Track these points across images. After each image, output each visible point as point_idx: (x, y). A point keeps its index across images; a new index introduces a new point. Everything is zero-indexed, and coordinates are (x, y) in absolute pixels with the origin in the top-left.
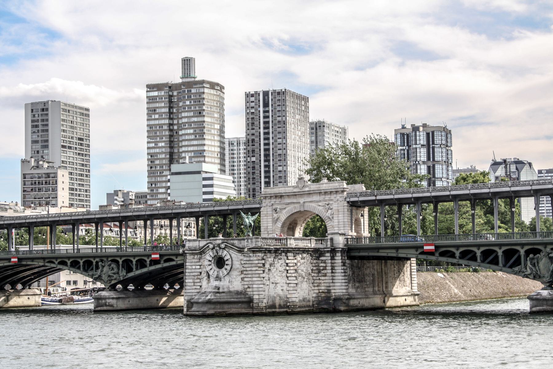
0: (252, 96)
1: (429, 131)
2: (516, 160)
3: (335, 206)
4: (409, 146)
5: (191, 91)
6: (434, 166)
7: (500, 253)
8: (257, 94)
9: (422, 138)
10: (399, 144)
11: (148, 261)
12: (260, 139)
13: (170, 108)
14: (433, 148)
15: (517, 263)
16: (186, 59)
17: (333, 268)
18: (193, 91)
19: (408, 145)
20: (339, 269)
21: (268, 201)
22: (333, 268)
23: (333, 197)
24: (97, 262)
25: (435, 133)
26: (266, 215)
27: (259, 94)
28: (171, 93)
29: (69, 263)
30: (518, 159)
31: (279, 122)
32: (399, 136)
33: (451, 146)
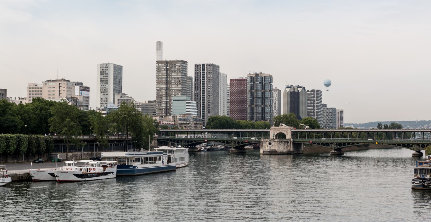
0: (198, 65)
1: (263, 76)
2: (298, 86)
3: (288, 132)
4: (254, 83)
5: (176, 64)
6: (265, 92)
7: (325, 143)
8: (200, 65)
9: (260, 80)
10: (249, 81)
11: (244, 142)
12: (201, 84)
13: (167, 71)
14: (265, 84)
15: (328, 145)
16: (158, 42)
17: (291, 145)
18: (177, 64)
19: (253, 82)
20: (292, 146)
21: (272, 130)
22: (291, 145)
23: (288, 130)
24: (230, 142)
25: (266, 77)
26: (272, 133)
27: (201, 65)
28: (167, 65)
29: (222, 142)
30: (299, 86)
31: (209, 77)
32: (249, 77)
33: (272, 83)
